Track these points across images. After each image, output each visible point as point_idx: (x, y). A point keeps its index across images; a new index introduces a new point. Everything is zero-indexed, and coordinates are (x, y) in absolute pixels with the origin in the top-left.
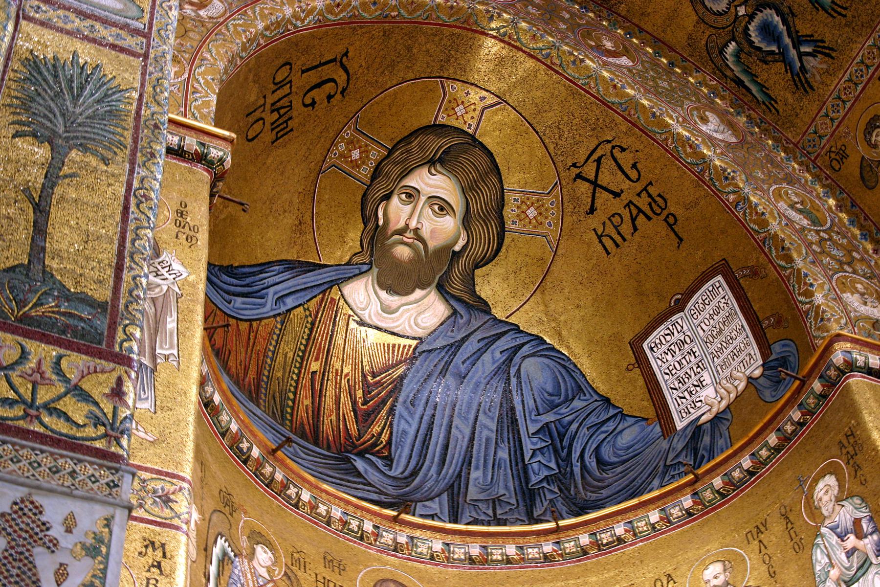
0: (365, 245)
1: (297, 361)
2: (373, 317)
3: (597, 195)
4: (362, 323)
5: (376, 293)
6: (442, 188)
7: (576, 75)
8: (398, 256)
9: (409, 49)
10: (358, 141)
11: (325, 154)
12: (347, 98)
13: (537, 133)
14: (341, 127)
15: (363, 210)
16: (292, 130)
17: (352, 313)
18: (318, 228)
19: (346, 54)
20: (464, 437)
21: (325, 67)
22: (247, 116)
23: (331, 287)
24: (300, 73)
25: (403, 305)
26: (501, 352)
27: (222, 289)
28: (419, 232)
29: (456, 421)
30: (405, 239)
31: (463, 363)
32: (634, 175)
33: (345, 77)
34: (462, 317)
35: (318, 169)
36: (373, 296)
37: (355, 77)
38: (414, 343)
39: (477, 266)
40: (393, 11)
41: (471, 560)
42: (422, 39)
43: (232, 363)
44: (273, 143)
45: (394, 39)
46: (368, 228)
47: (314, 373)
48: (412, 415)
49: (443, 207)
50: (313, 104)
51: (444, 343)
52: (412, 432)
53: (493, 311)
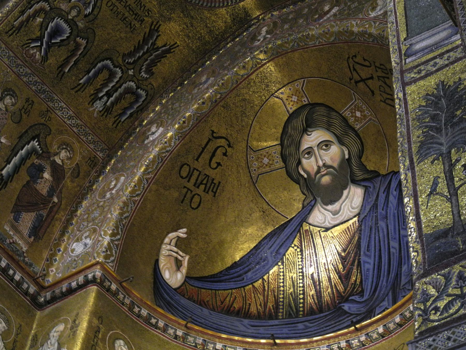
0: (306, 192)
1: (299, 276)
2: (331, 222)
3: (368, 84)
4: (327, 229)
5: (326, 209)
6: (319, 137)
7: (313, 42)
8: (325, 183)
9: (244, 100)
10: (261, 155)
11: (249, 175)
12: (235, 146)
13: (327, 79)
14: (245, 158)
15: (292, 179)
16: (220, 183)
17: (319, 229)
18: (275, 206)
19: (213, 132)
20: (396, 250)
21: (208, 146)
22: (182, 202)
23: (302, 226)
24: (196, 162)
25: (342, 204)
26: (395, 190)
27: (232, 278)
28: (326, 164)
29: (392, 243)
30: (322, 173)
31: (383, 210)
32: (367, 63)
33: (223, 140)
34: (370, 187)
35: (252, 183)
36: (326, 212)
37: (229, 136)
38: (356, 219)
39: (360, 157)
40: (216, 96)
41: (399, 325)
42: (245, 91)
43: (253, 309)
44: (214, 196)
45: (231, 105)
46: (301, 184)
47: (312, 275)
48: (369, 257)
49: (326, 144)
50: (219, 164)
51: (369, 207)
52: (371, 267)
53: (381, 172)
